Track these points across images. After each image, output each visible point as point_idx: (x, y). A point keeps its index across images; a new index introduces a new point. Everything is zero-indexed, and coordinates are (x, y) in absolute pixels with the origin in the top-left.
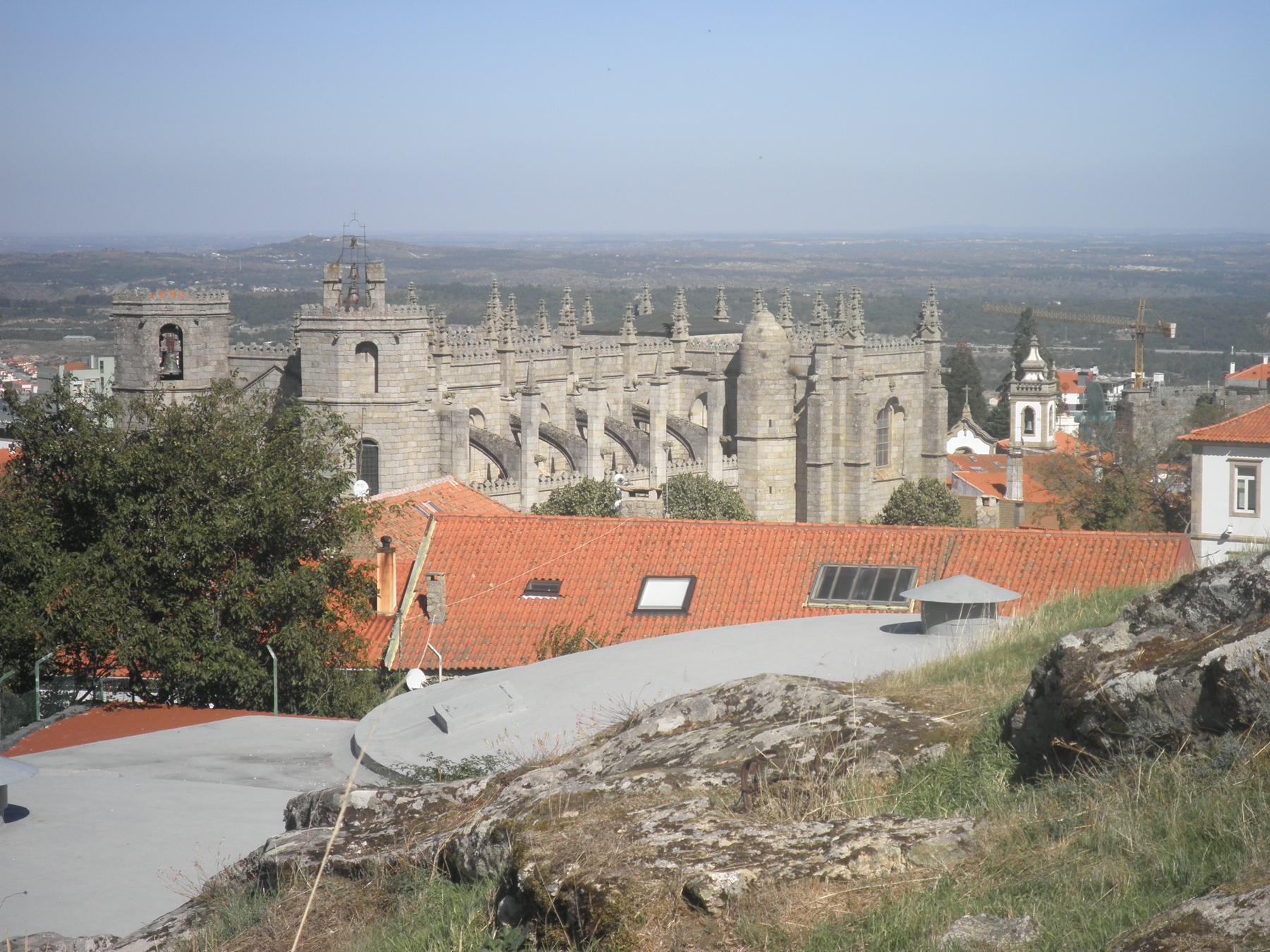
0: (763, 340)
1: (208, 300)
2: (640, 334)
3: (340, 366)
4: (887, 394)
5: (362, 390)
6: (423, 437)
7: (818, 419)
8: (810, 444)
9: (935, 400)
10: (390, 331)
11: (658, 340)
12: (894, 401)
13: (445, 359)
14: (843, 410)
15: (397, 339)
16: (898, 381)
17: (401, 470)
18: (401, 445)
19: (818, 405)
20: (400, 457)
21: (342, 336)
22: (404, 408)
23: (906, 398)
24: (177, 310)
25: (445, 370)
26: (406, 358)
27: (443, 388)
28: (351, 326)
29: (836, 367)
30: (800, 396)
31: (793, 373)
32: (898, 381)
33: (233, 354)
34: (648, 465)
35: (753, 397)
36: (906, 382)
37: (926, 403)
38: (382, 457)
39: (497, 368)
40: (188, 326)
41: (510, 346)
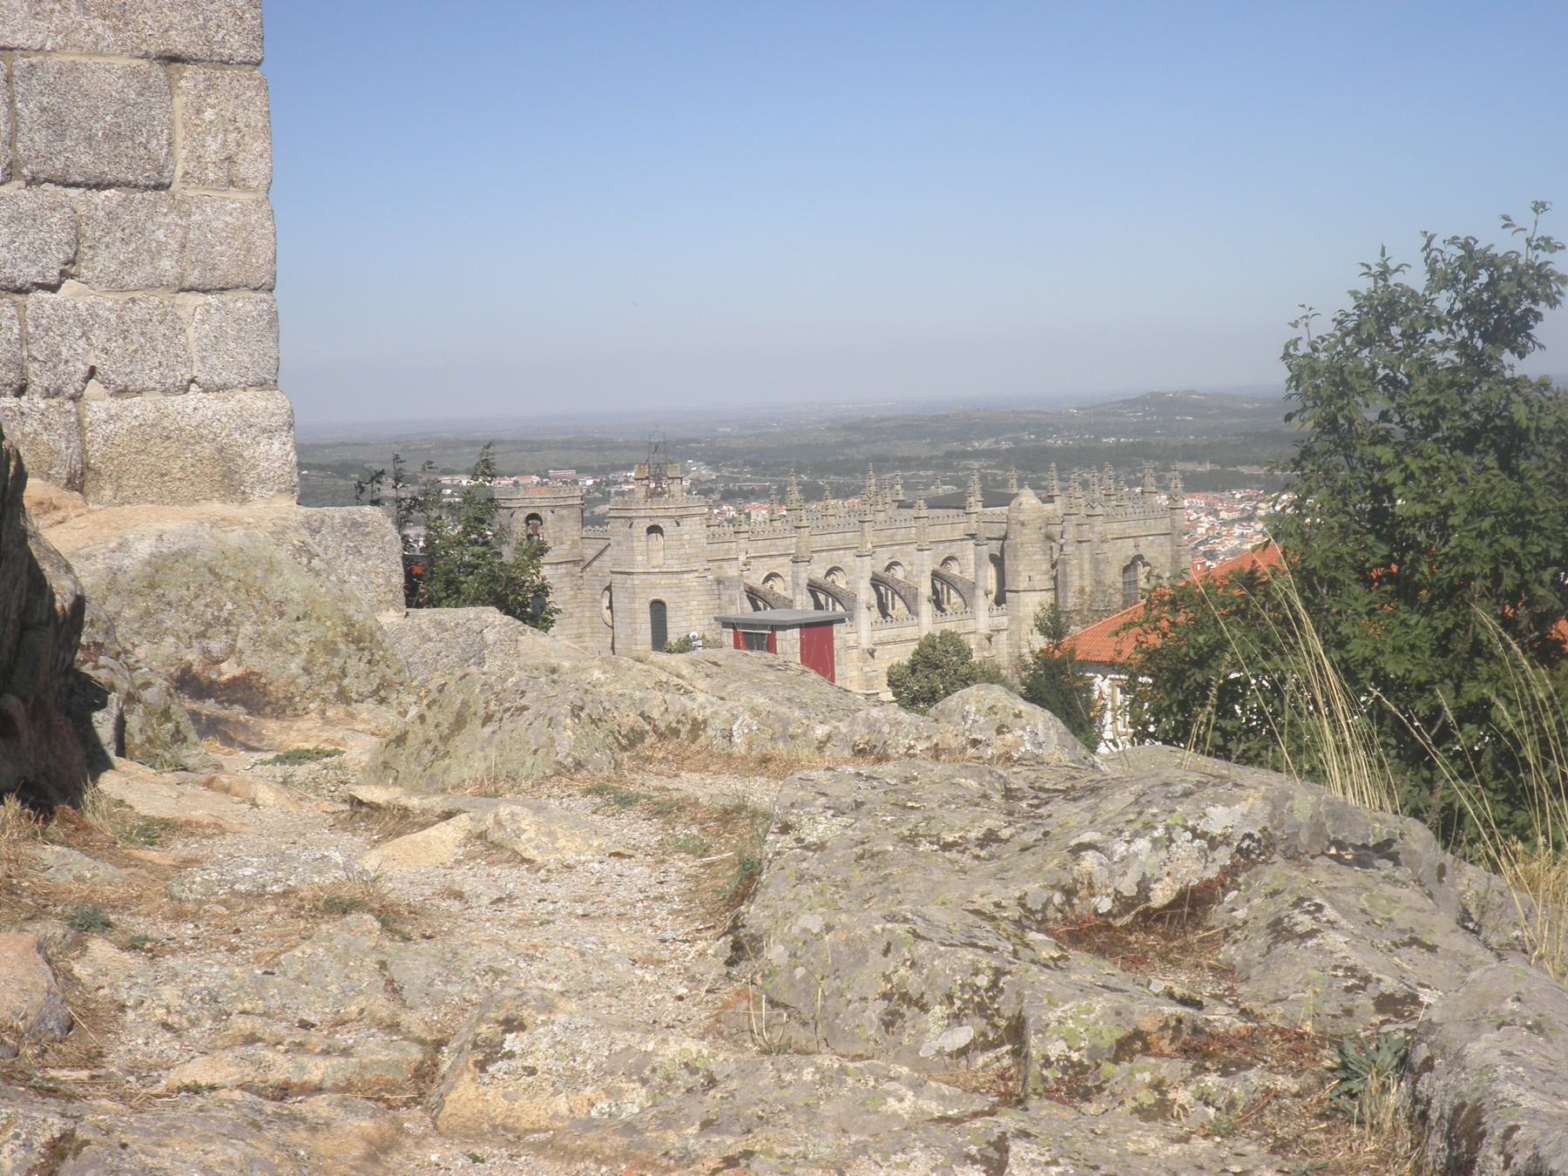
0: (1022, 511)
1: (562, 494)
2: (930, 507)
3: (635, 544)
4: (1132, 553)
5: (654, 562)
6: (701, 598)
7: (1065, 574)
8: (1061, 595)
9: (1179, 557)
10: (672, 517)
11: (952, 512)
12: (1140, 557)
13: (742, 535)
14: (1087, 566)
15: (678, 524)
16: (1143, 542)
17: (684, 624)
18: (683, 604)
19: (1065, 563)
20: (684, 613)
21: (636, 521)
22: (686, 576)
23: (1152, 555)
24: (537, 502)
25: (743, 544)
26: (686, 537)
27: (742, 558)
28: (642, 513)
29: (1080, 532)
30: (1055, 556)
31: (1049, 538)
32: (1143, 542)
33: (584, 535)
34: (917, 614)
35: (1016, 557)
36: (1152, 542)
37: (1173, 557)
38: (669, 614)
39: (794, 540)
40: (546, 515)
41: (804, 523)
